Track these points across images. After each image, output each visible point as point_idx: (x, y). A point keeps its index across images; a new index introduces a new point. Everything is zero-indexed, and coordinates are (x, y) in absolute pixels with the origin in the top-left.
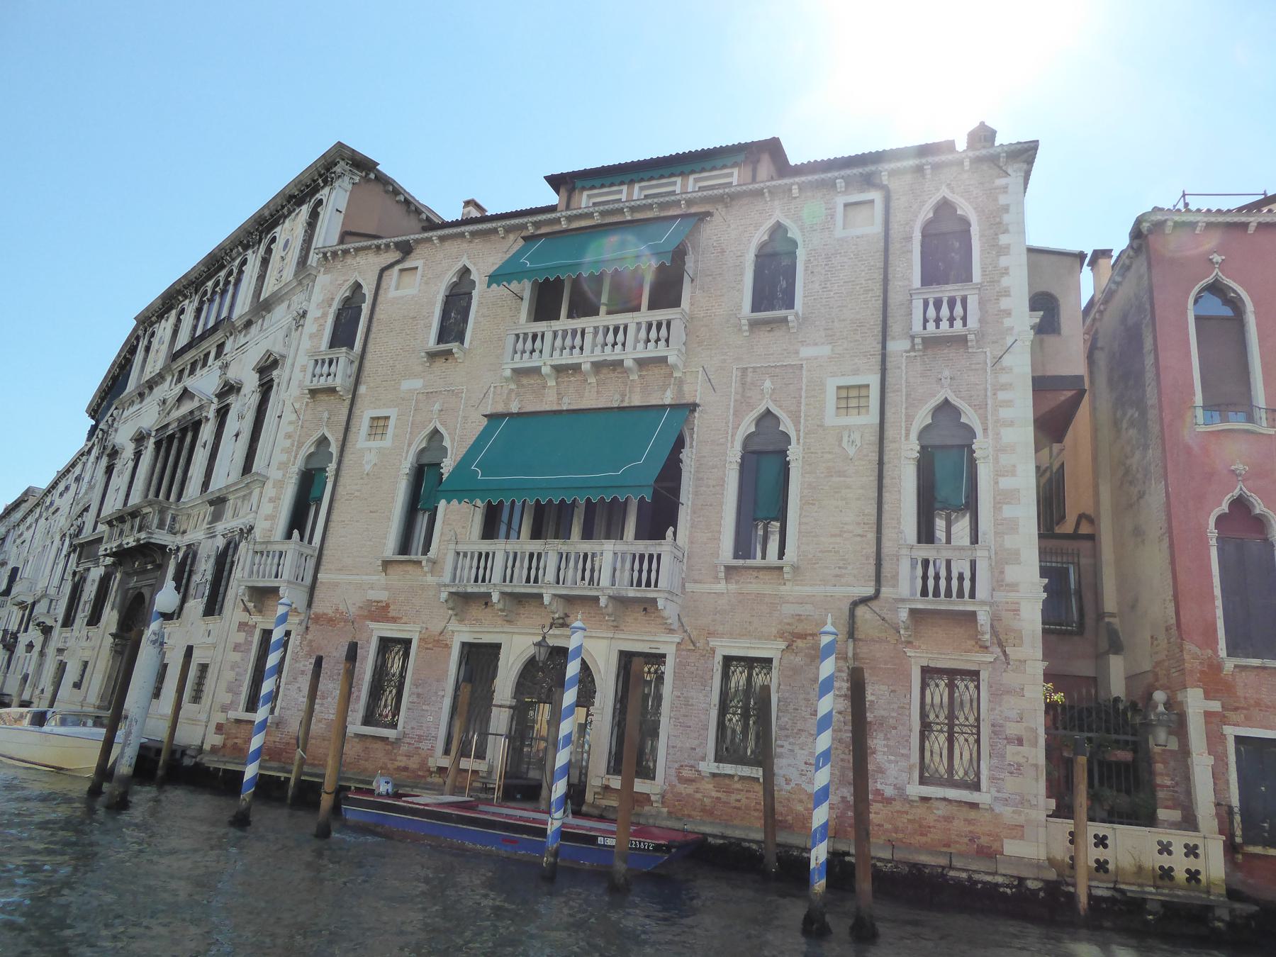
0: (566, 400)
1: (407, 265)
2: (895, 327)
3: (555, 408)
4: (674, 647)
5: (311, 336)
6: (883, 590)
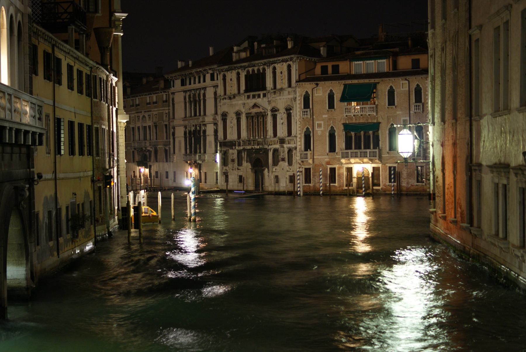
5: (299, 104)
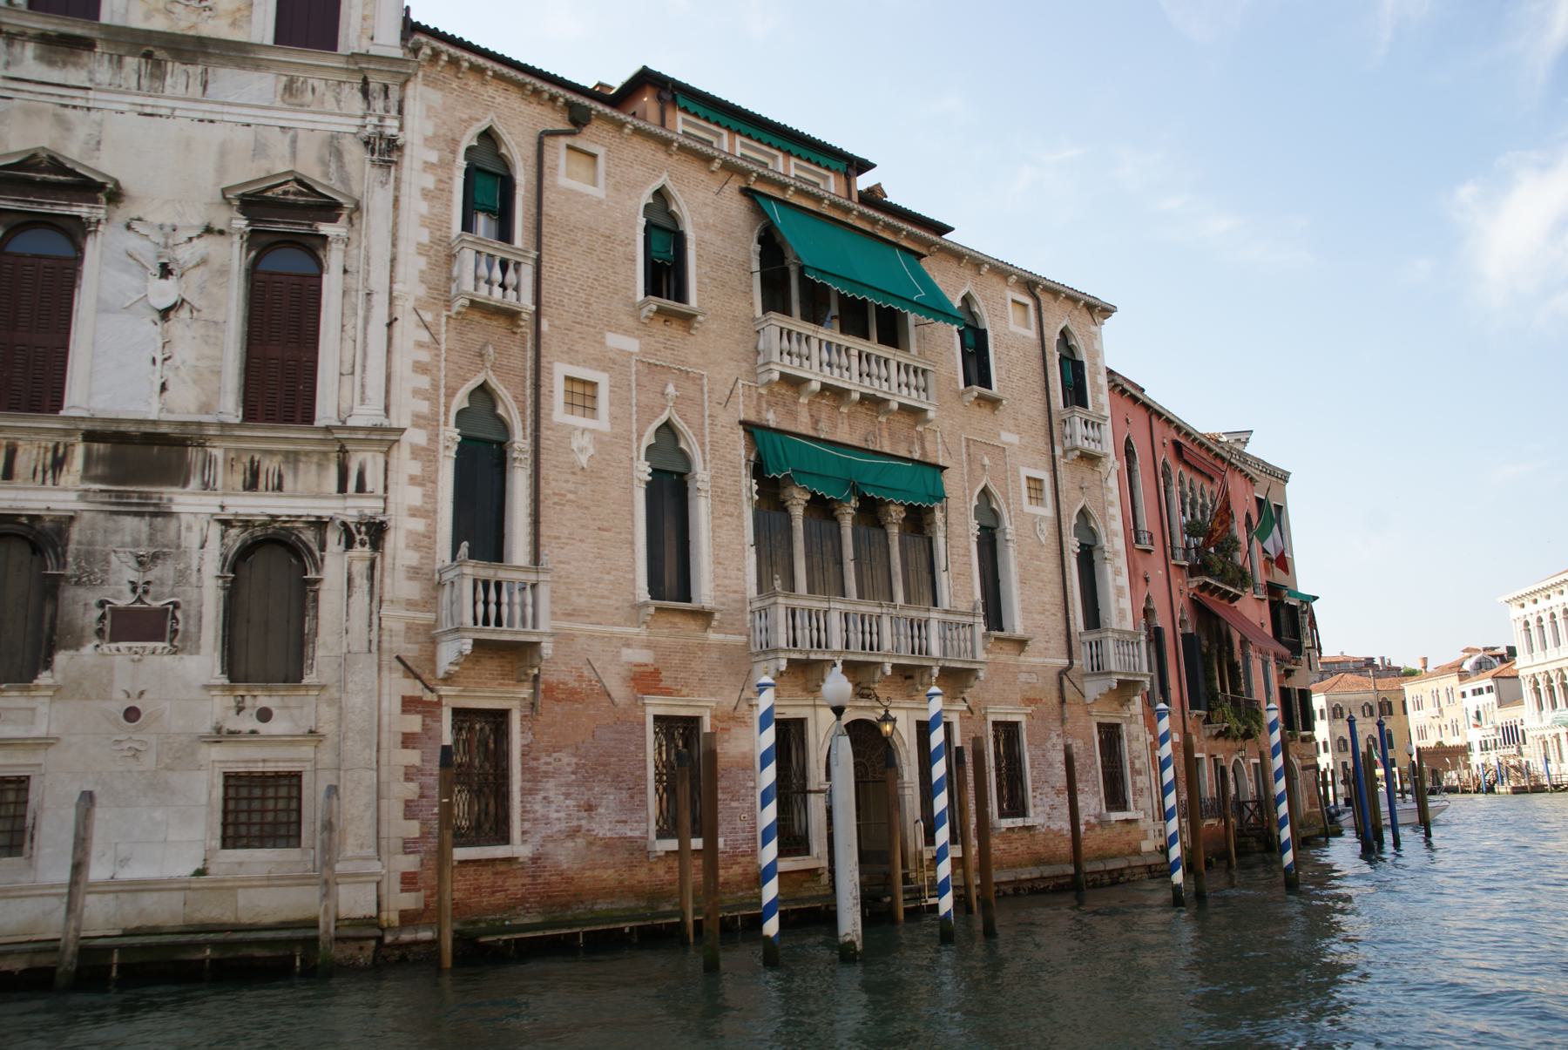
0: (822, 425)
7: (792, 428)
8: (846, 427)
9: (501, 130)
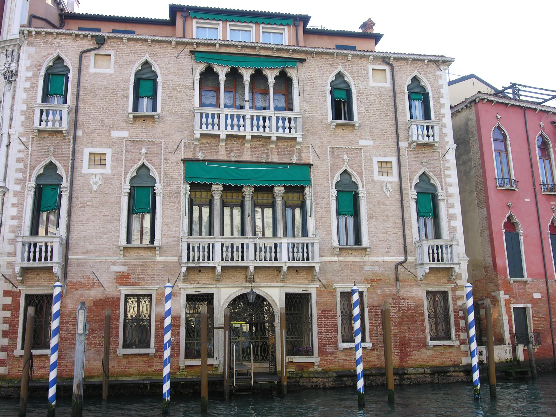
1: (101, 52)
2: (401, 136)
3: (226, 158)
4: (315, 289)
6: (409, 258)
7: (215, 158)
8: (249, 153)
9: (62, 56)
